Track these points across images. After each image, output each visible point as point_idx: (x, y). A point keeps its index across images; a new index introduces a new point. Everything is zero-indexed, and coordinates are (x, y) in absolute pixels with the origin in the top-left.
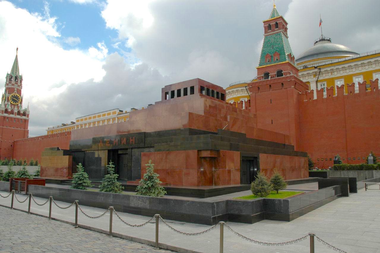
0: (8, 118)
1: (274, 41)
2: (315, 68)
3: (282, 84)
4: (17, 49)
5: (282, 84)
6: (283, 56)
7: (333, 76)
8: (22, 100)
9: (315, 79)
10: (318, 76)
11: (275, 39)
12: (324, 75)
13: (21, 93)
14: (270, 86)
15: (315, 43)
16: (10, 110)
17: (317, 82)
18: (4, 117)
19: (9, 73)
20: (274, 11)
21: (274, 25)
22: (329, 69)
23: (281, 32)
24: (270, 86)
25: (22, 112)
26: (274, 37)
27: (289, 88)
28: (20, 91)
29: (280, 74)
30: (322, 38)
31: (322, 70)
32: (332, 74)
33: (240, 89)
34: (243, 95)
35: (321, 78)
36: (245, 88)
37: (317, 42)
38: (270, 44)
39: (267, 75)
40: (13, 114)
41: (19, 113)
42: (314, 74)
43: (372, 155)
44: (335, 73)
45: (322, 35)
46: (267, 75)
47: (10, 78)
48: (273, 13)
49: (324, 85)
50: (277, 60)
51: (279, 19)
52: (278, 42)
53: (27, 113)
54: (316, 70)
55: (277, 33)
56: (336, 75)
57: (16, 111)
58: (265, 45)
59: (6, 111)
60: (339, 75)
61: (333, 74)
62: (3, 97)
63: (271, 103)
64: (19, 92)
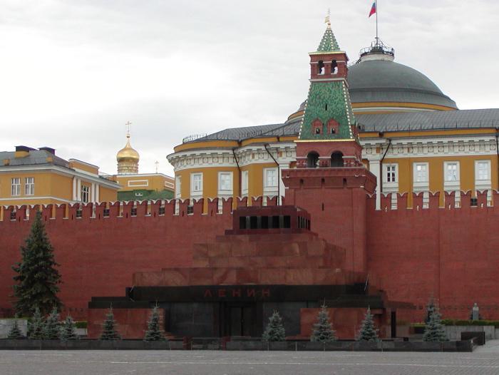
1: (330, 97)
2: (381, 135)
3: (345, 180)
5: (345, 180)
6: (346, 128)
7: (411, 156)
9: (379, 157)
10: (385, 151)
11: (331, 92)
12: (395, 151)
14: (323, 180)
15: (362, 55)
17: (382, 161)
20: (329, 37)
21: (330, 66)
22: (405, 142)
23: (342, 81)
24: (323, 180)
26: (329, 89)
27: (357, 189)
29: (337, 157)
30: (377, 44)
31: (394, 142)
32: (408, 151)
33: (220, 152)
34: (226, 164)
35: (389, 156)
36: (231, 152)
37: (365, 54)
38: (321, 101)
39: (313, 157)
42: (379, 146)
43: (478, 306)
44: (415, 151)
45: (377, 38)
46: (313, 157)
48: (327, 40)
49: (393, 168)
50: (333, 132)
51: (340, 57)
52: (337, 101)
54: (383, 141)
55: (335, 81)
56: (416, 154)
58: (312, 99)
60: (420, 155)
61: (411, 151)
63: (323, 209)
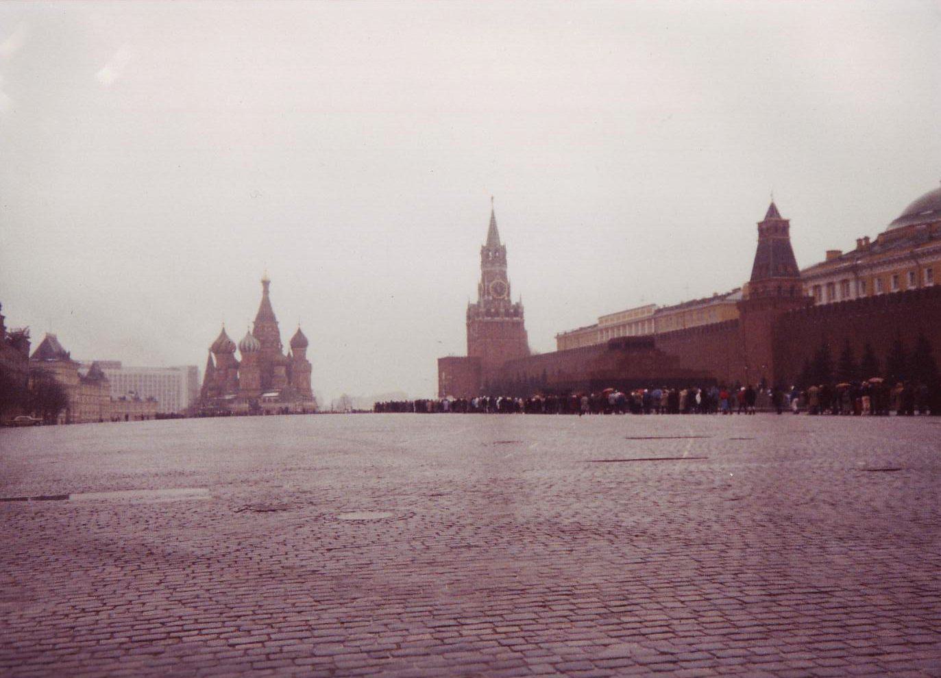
0: (492, 323)
4: (492, 198)
8: (509, 288)
13: (506, 279)
16: (493, 310)
18: (487, 323)
19: (485, 244)
25: (512, 311)
28: (505, 273)
40: (498, 316)
41: (507, 314)
47: (485, 252)
53: (520, 310)
57: (502, 310)
59: (488, 313)
62: (480, 289)
64: (503, 275)
